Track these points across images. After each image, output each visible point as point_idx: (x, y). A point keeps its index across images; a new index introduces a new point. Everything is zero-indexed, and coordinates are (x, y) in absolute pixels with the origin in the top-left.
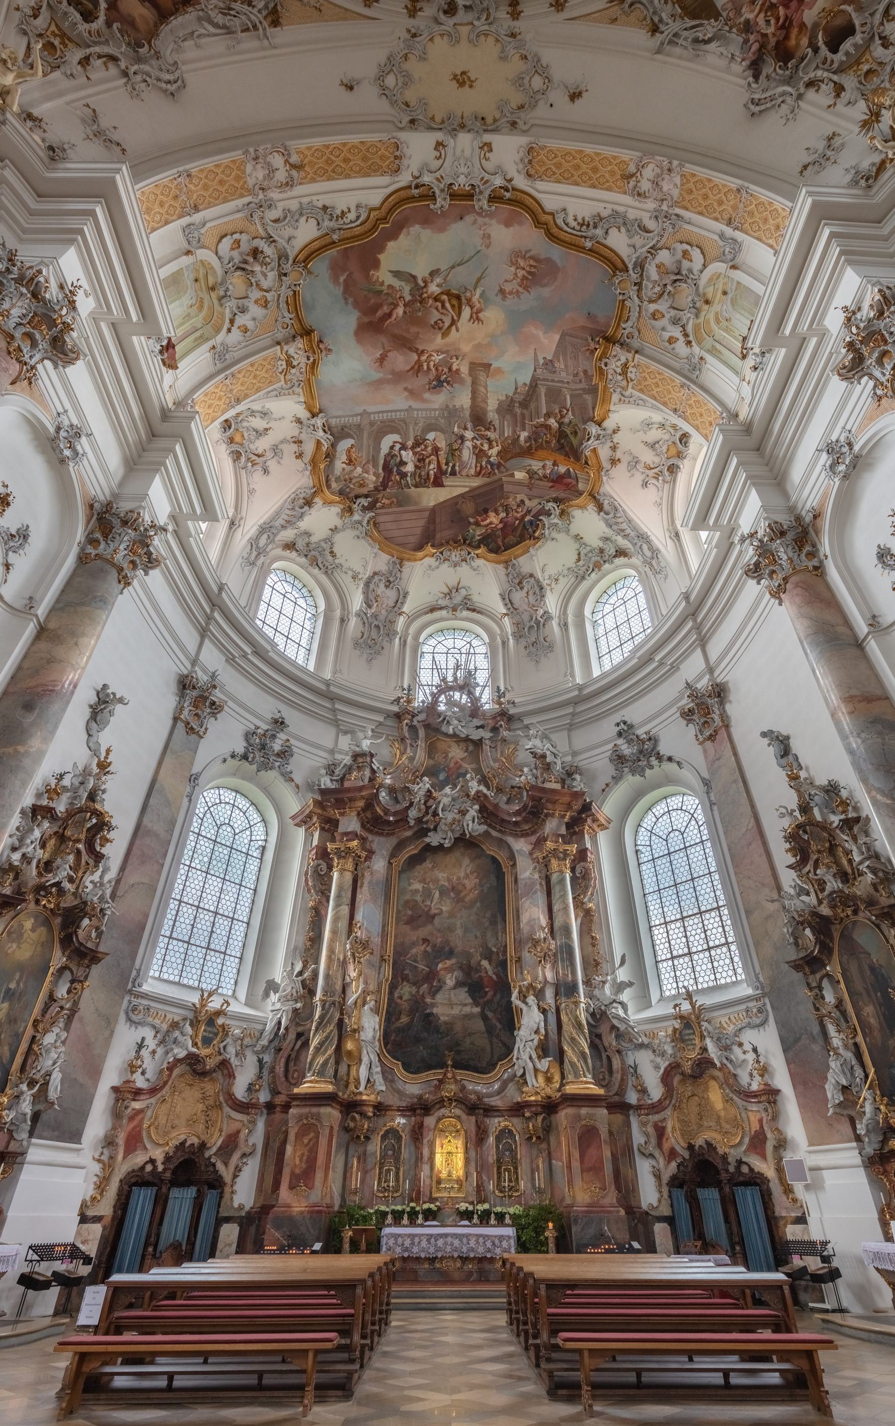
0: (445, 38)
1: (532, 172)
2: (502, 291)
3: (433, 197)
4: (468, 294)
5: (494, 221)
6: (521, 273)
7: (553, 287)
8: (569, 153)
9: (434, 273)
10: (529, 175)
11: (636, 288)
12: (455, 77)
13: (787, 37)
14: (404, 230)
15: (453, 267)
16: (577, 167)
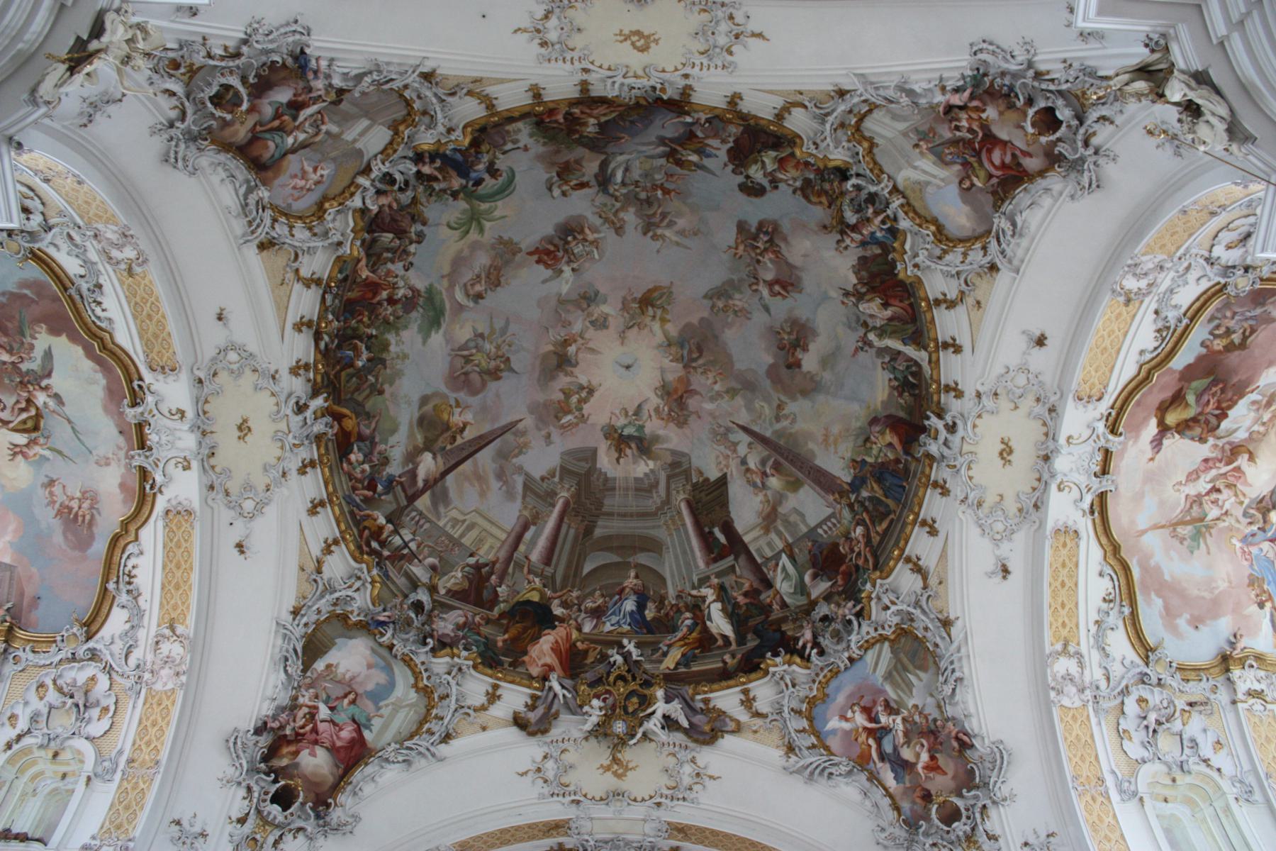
0: (275, 408)
1: (171, 516)
2: (51, 483)
3: (134, 404)
4: (42, 441)
5: (123, 470)
6: (75, 504)
7: (64, 547)
8: (190, 556)
9: (57, 397)
10: (167, 512)
11: (70, 656)
12: (245, 421)
13: (289, 743)
14: (97, 367)
15: (69, 421)
16: (178, 567)
